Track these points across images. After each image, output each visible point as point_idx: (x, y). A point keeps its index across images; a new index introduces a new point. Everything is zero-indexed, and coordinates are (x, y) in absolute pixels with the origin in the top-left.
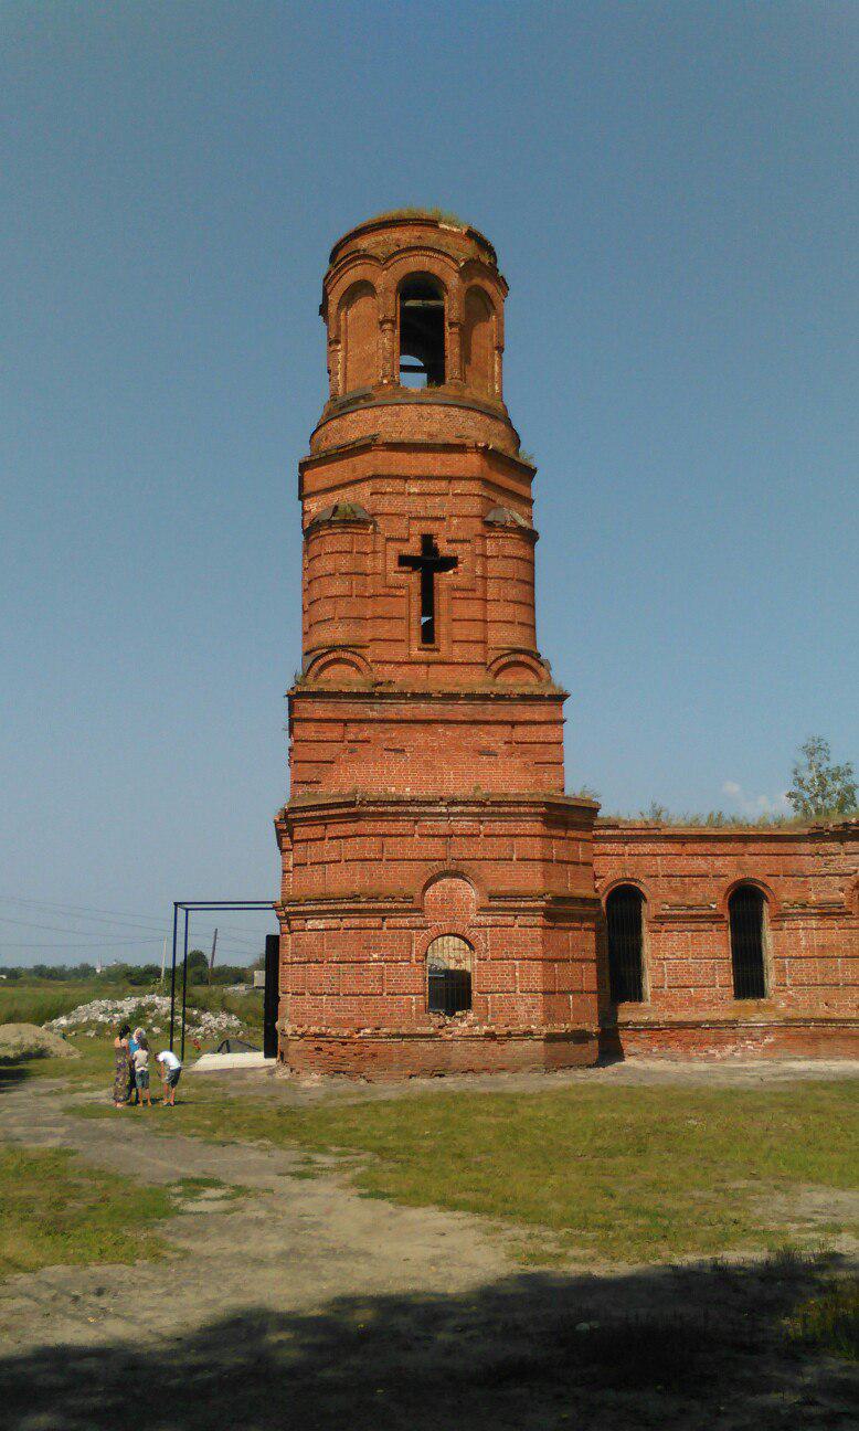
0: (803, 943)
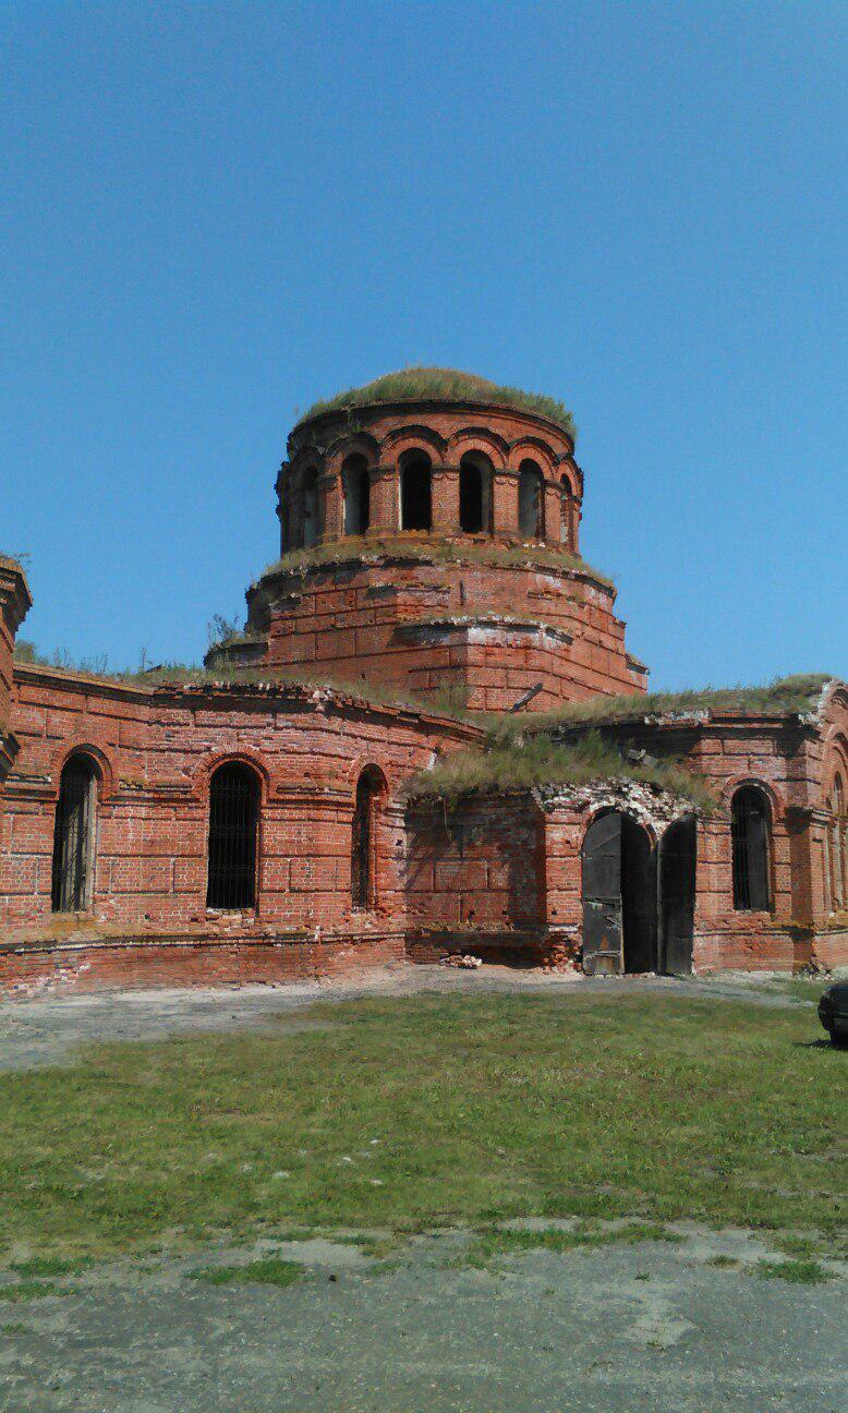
0: (131, 836)
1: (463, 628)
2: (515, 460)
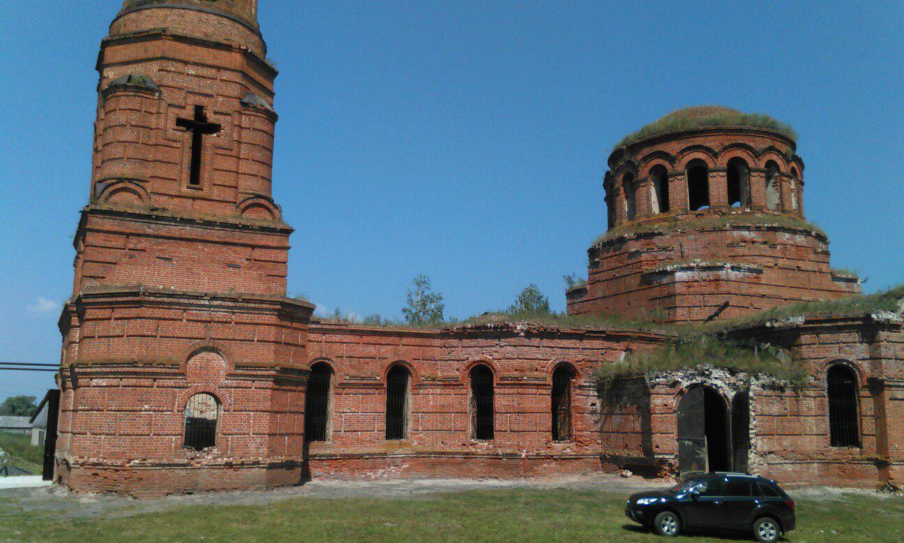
0: (431, 403)
1: (672, 273)
2: (723, 161)
